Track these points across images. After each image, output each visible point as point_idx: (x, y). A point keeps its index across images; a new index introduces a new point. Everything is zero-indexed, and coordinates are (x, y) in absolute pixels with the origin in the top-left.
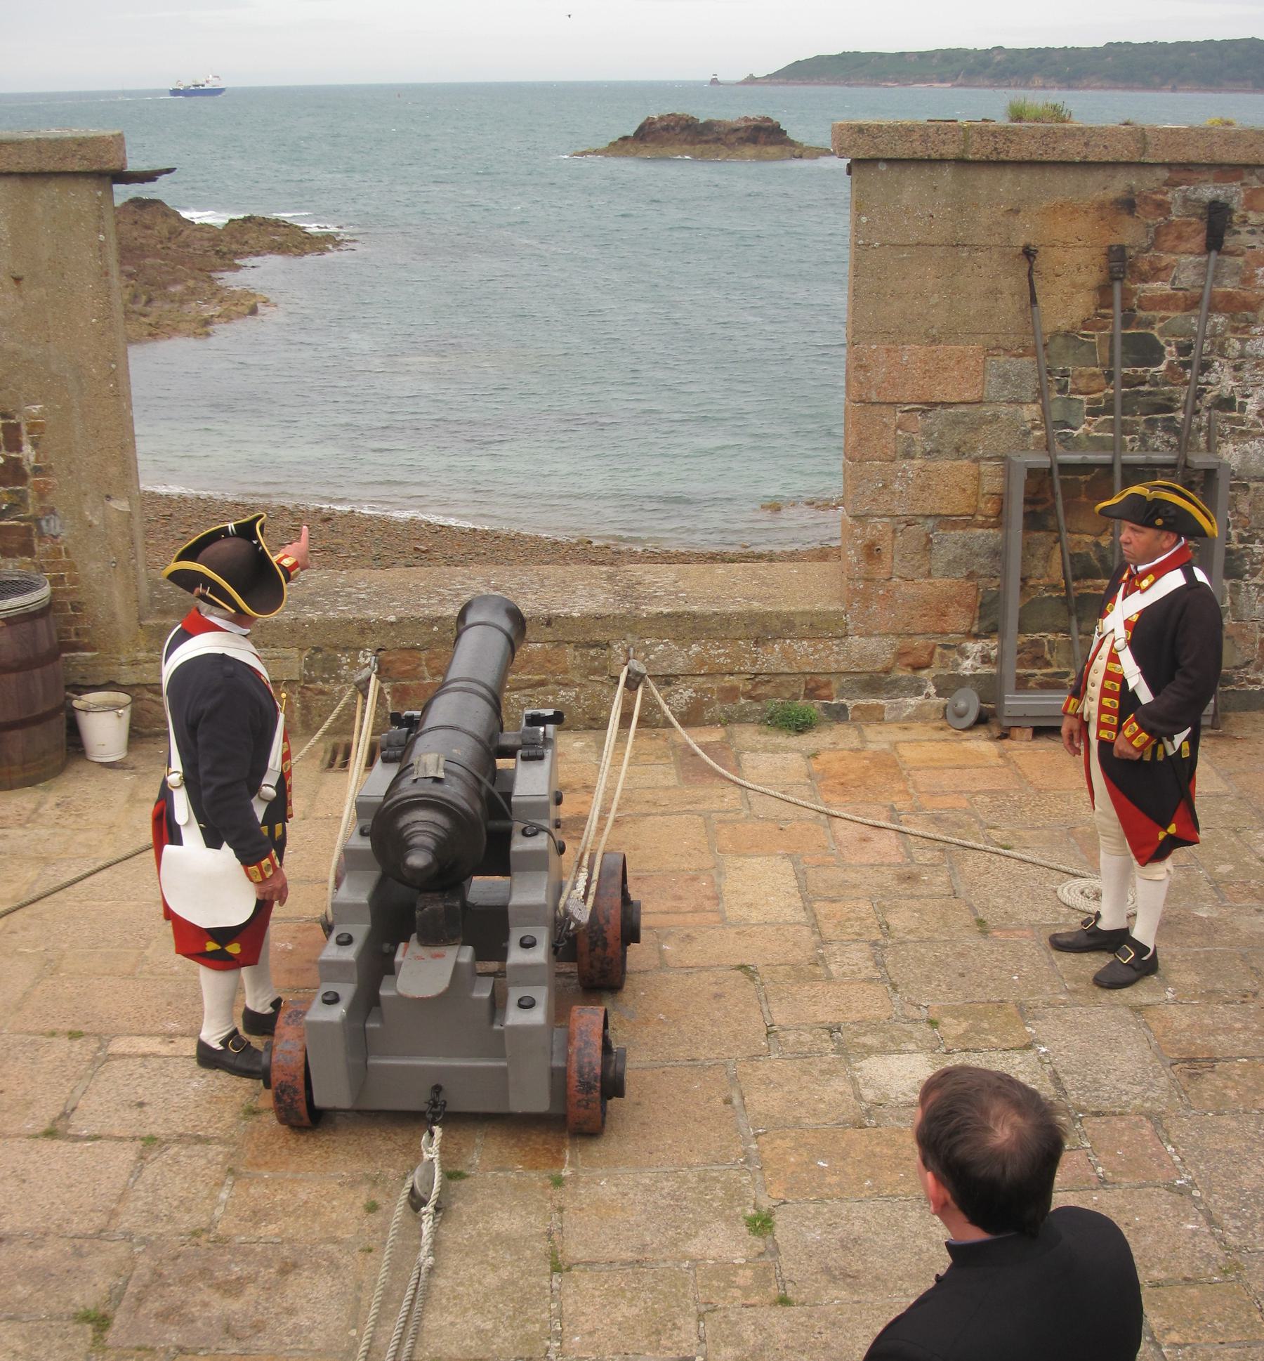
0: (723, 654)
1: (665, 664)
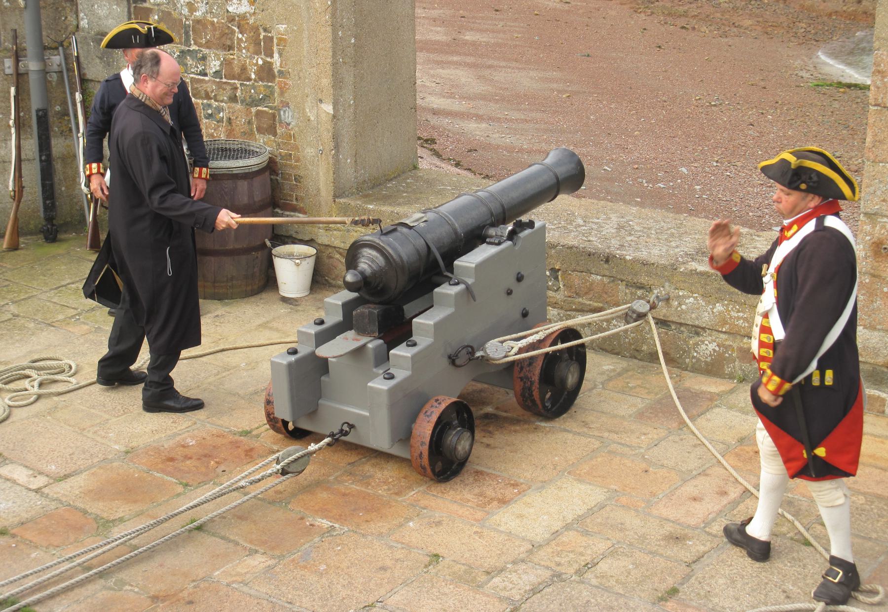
0: (742, 318)
1: (693, 316)
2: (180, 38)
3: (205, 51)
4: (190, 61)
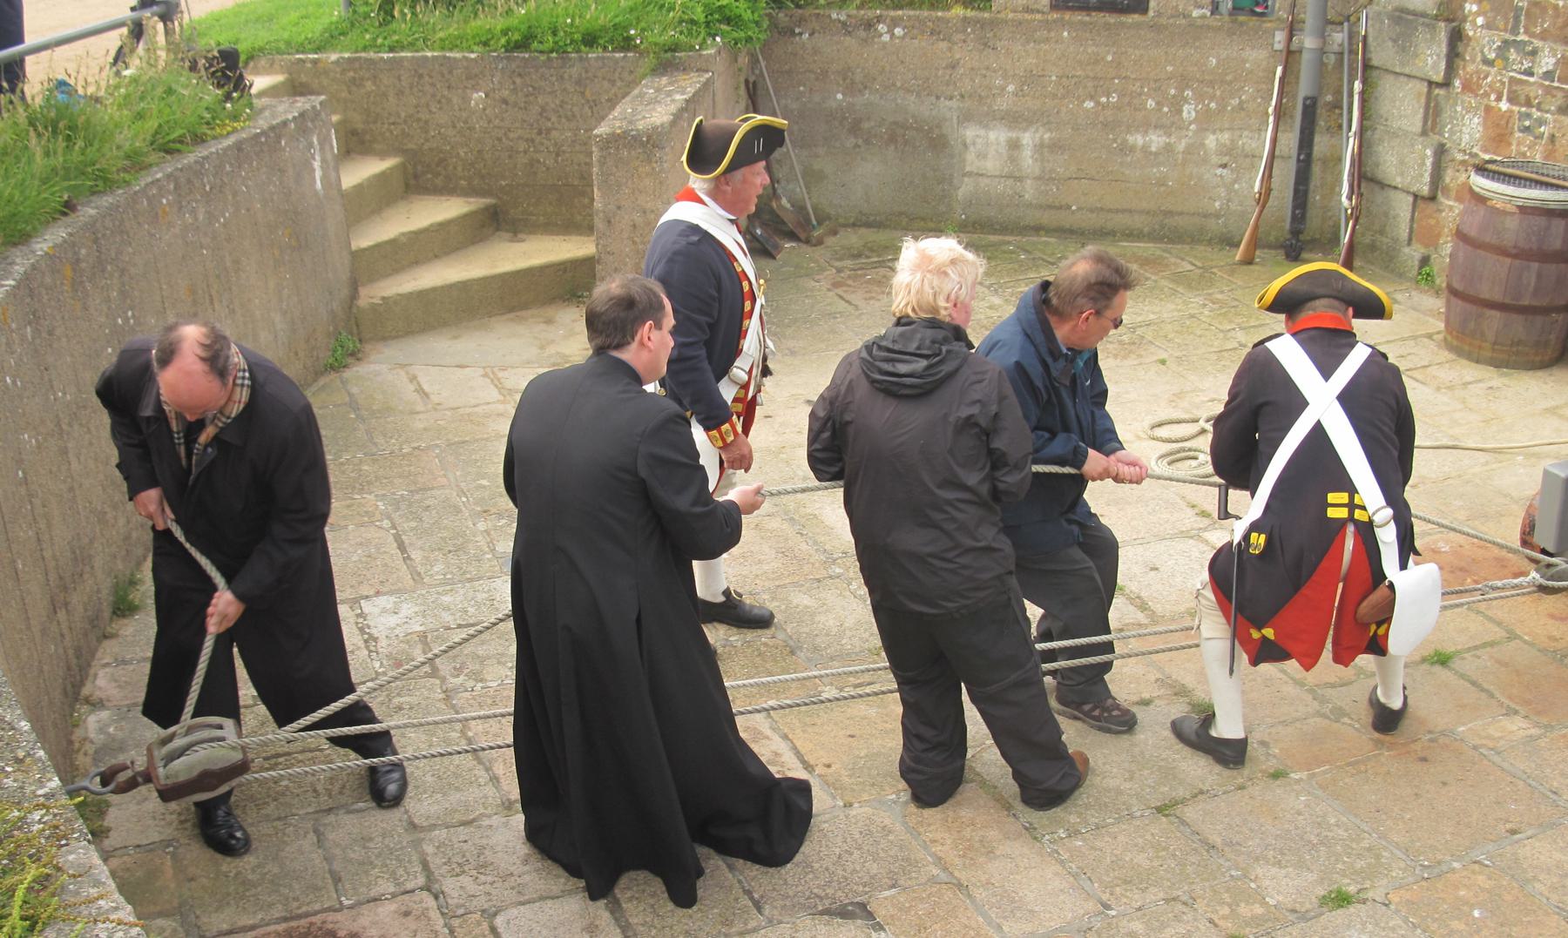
2: (1506, 24)
3: (1538, 43)
4: (1513, 54)
